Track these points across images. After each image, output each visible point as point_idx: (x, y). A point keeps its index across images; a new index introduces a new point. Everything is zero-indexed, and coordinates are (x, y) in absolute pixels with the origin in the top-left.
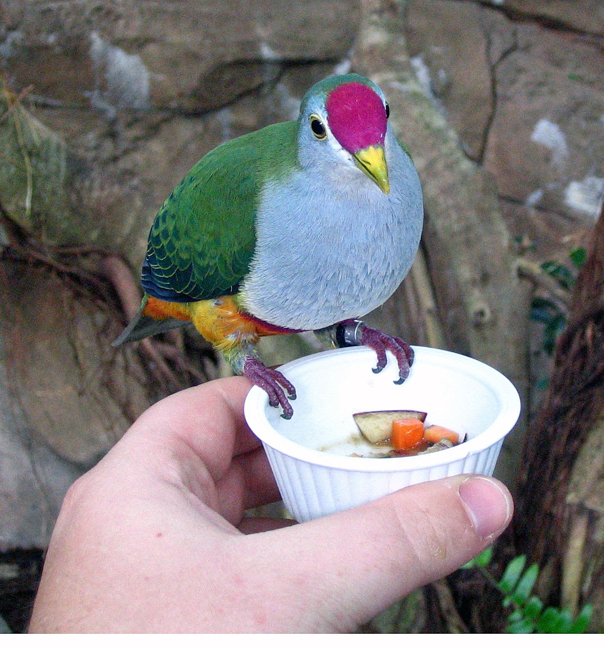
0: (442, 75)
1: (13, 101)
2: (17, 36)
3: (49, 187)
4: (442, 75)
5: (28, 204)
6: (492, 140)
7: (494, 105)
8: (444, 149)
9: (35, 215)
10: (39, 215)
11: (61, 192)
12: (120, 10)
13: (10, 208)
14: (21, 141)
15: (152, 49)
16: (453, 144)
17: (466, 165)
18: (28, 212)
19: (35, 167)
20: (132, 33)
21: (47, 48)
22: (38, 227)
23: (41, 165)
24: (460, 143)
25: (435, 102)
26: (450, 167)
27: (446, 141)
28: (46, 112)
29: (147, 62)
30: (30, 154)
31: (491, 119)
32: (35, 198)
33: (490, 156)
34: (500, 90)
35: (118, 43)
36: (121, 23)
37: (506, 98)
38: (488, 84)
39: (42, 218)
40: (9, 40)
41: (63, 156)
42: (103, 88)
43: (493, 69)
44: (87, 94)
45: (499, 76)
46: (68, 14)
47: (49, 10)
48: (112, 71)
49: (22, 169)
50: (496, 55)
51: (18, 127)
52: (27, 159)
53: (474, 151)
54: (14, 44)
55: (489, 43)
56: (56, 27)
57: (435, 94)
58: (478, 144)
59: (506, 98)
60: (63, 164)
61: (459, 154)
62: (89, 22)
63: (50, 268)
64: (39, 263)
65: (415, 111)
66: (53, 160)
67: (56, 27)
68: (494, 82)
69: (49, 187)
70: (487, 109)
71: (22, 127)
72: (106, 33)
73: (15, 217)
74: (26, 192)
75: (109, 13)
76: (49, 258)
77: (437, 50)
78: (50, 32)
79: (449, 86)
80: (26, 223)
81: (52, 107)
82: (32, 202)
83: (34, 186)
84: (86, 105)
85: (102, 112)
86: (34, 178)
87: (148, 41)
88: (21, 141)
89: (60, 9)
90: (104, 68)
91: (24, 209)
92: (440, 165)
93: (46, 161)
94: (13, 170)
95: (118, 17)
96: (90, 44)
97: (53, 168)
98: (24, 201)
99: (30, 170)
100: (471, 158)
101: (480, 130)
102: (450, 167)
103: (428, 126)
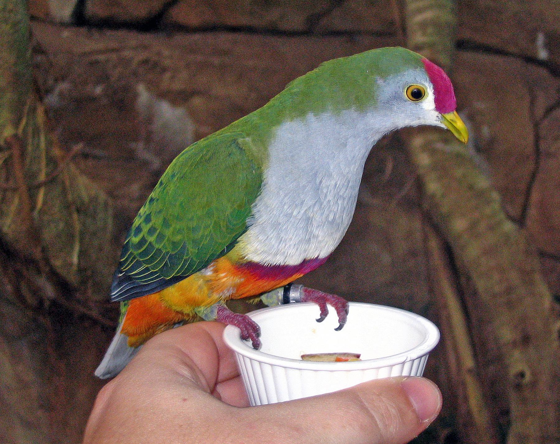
0: (486, 131)
1: (63, 158)
2: (63, 86)
3: (96, 242)
4: (486, 131)
5: (75, 259)
6: (535, 196)
7: (537, 163)
8: (488, 211)
9: (81, 270)
10: (85, 270)
11: (107, 247)
12: (167, 63)
13: (57, 263)
14: (70, 198)
15: (197, 101)
16: (496, 206)
17: (509, 226)
18: (75, 268)
19: (84, 224)
20: (177, 86)
21: (93, 99)
22: (84, 282)
23: (89, 221)
24: (503, 208)
25: (478, 159)
26: (491, 228)
27: (488, 202)
28: (90, 163)
29: (192, 114)
30: (78, 211)
31: (534, 176)
32: (82, 254)
33: (533, 212)
34: (543, 146)
35: (163, 95)
36: (168, 75)
37: (549, 155)
38: (531, 139)
39: (89, 273)
40: (57, 91)
41: (110, 211)
42: (148, 139)
43: (536, 125)
44: (133, 145)
45: (543, 133)
46: (115, 66)
47: (97, 62)
48: (157, 126)
49: (69, 225)
50: (540, 112)
51: (68, 183)
52: (75, 216)
53: (515, 211)
54: (61, 94)
55: (533, 102)
56: (104, 78)
57: (478, 149)
58: (520, 200)
59: (549, 155)
60: (110, 221)
61: (502, 216)
62: (135, 74)
63: (95, 322)
64: (83, 317)
65: (459, 172)
66: (101, 215)
67: (104, 78)
68: (537, 138)
69: (96, 242)
70: (530, 166)
71: (71, 184)
72: (152, 85)
73: (63, 272)
74: (72, 248)
75: (156, 64)
76: (94, 313)
77: (480, 105)
78: (98, 83)
79: (492, 141)
80: (73, 278)
81: (95, 157)
82: (79, 256)
83: (81, 243)
84: (131, 156)
85: (145, 163)
86: (82, 233)
87: (194, 93)
88: (70, 198)
89: (108, 61)
90: (150, 120)
91: (71, 264)
92: (482, 226)
93: (94, 217)
94: (61, 225)
95: (164, 70)
96: (136, 96)
97: (100, 224)
98: (70, 253)
99: (78, 226)
100: (512, 219)
101: (522, 186)
102: (491, 228)
103: (471, 187)
